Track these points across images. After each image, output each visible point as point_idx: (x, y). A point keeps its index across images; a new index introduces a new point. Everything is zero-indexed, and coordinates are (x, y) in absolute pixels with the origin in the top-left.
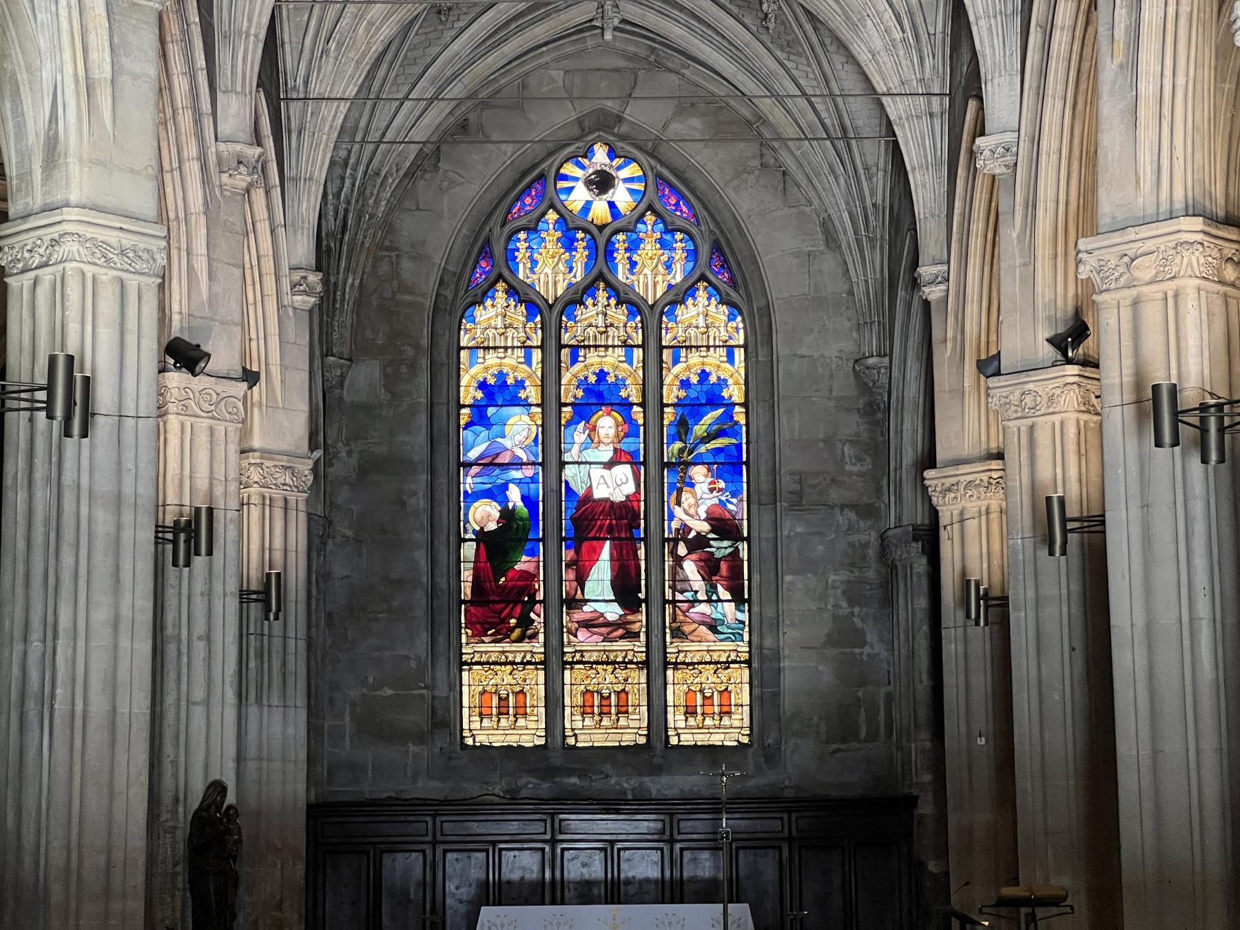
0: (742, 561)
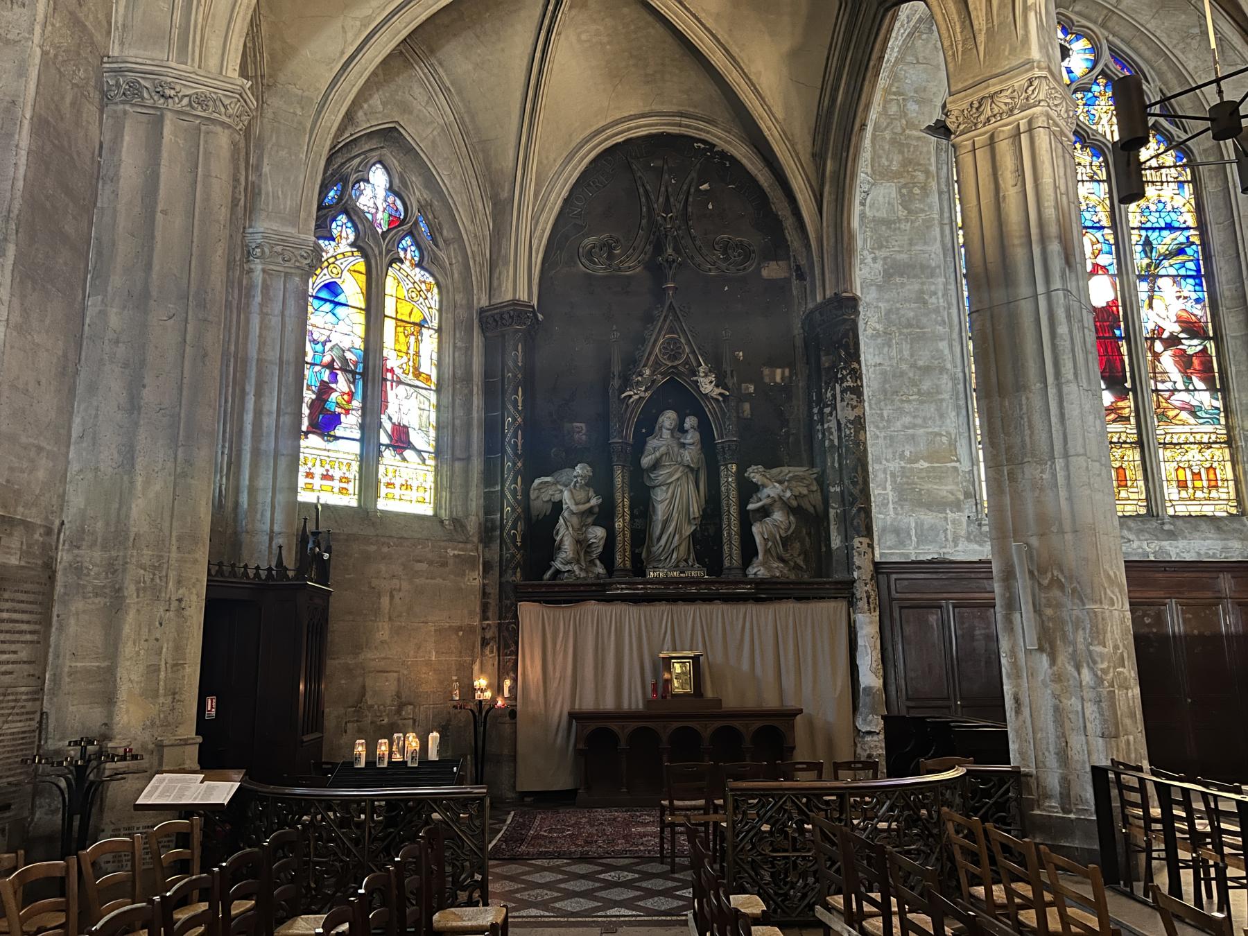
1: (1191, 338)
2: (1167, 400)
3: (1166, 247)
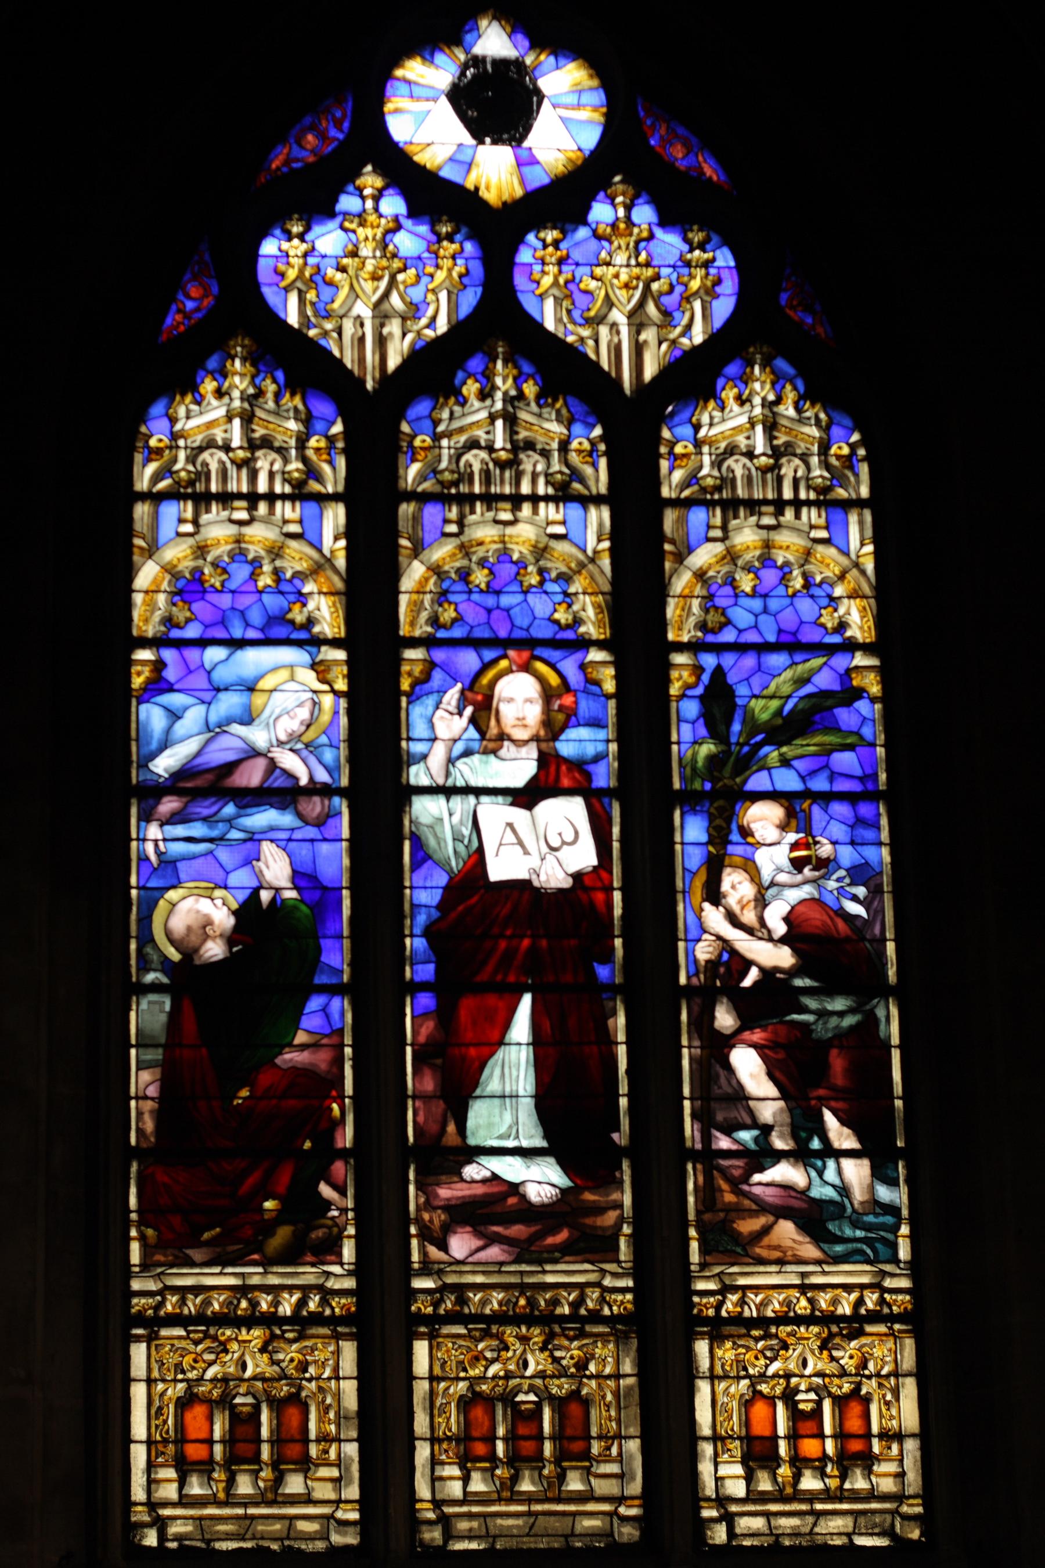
0: (887, 1047)
1: (827, 991)
2: (738, 1183)
3: (775, 704)
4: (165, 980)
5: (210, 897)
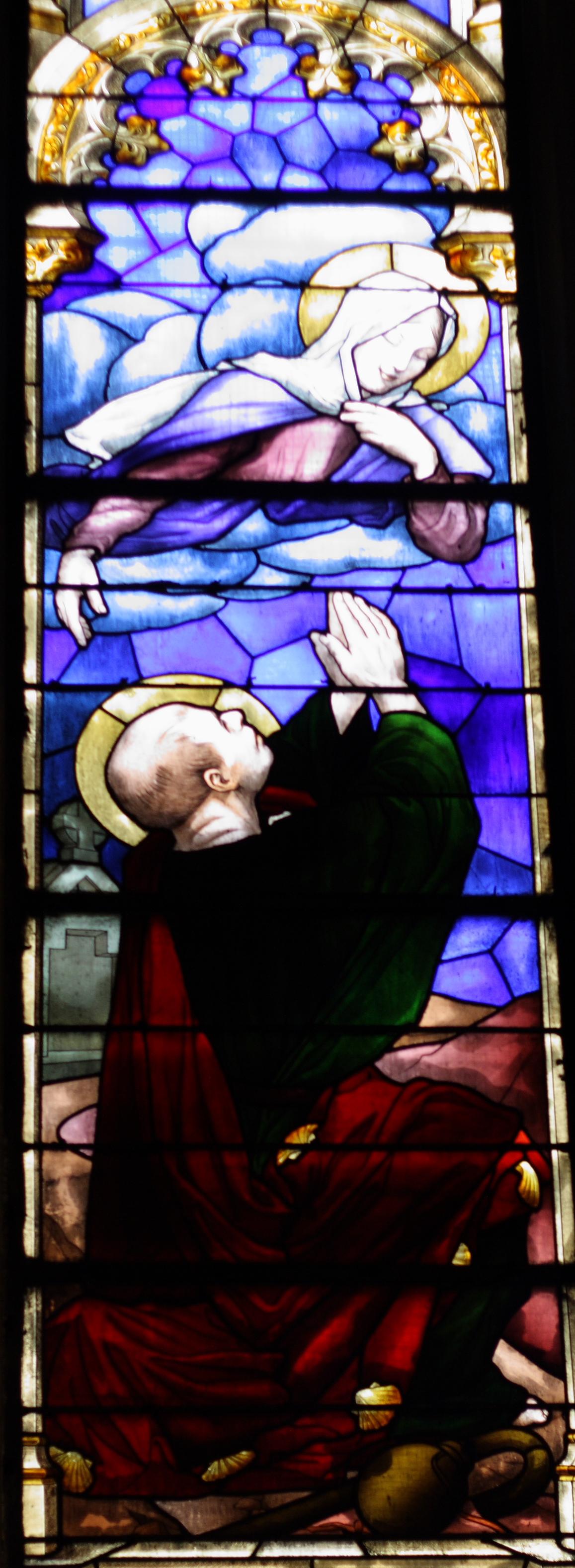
4: (107, 885)
5: (212, 708)
